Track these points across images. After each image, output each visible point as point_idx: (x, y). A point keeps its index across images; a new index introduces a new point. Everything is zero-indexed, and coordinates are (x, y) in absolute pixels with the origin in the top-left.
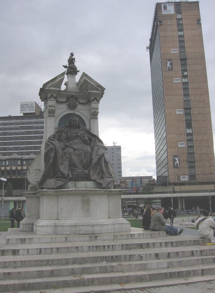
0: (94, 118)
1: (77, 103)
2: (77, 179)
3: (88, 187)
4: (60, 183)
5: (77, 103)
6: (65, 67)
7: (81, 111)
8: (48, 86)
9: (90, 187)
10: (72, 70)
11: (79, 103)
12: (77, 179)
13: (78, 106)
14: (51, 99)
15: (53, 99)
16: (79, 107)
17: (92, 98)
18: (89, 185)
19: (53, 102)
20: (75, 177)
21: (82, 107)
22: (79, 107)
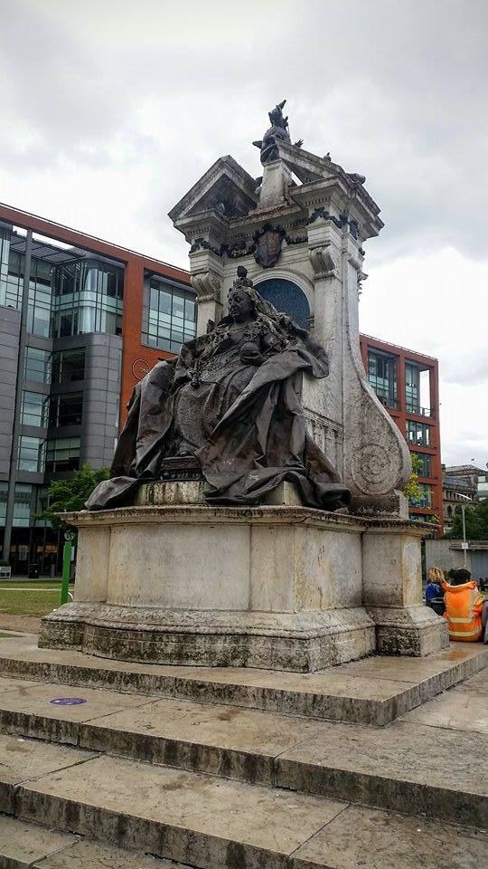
0: (325, 277)
1: (284, 244)
2: (173, 476)
3: (185, 499)
4: (118, 490)
5: (284, 244)
6: (299, 144)
7: (292, 267)
8: (181, 215)
9: (192, 499)
10: (274, 144)
11: (290, 242)
12: (173, 476)
13: (285, 254)
14: (198, 252)
15: (202, 249)
16: (289, 254)
17: (311, 212)
18: (190, 490)
19: (202, 258)
20: (169, 471)
21: (296, 252)
22: (289, 254)
